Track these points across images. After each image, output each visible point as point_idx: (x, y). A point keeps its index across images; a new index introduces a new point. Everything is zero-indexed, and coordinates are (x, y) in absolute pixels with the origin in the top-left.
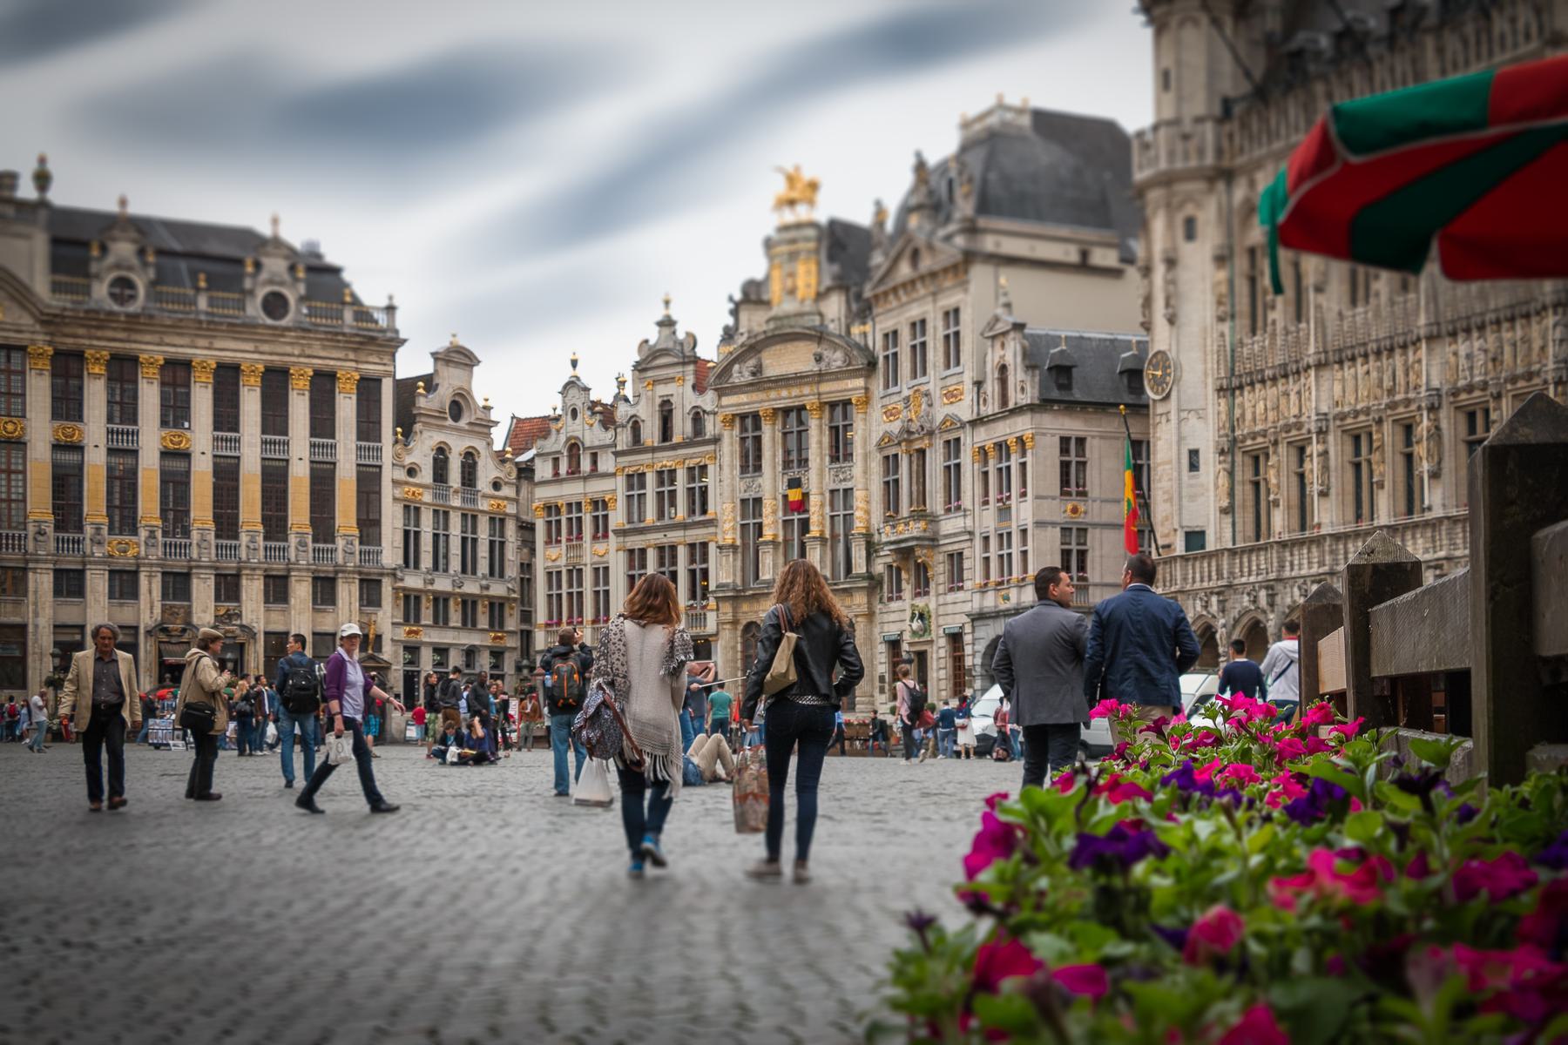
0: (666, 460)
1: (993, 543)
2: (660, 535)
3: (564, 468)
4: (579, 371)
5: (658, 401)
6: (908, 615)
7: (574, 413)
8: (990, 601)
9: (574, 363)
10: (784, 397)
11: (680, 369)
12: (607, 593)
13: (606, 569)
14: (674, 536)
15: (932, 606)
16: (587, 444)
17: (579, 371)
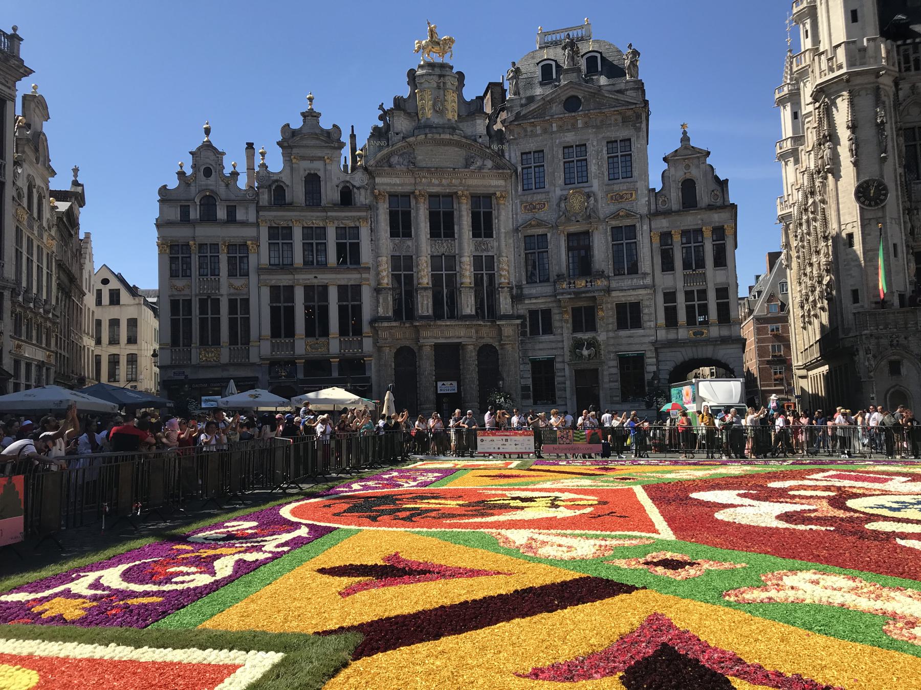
0: (314, 218)
1: (681, 299)
2: (312, 276)
3: (194, 214)
4: (211, 138)
5: (303, 174)
6: (567, 344)
7: (208, 172)
8: (683, 333)
9: (207, 131)
10: (436, 185)
11: (329, 151)
12: (247, 321)
13: (246, 302)
14: (323, 278)
15: (602, 337)
16: (223, 196)
17: (211, 138)
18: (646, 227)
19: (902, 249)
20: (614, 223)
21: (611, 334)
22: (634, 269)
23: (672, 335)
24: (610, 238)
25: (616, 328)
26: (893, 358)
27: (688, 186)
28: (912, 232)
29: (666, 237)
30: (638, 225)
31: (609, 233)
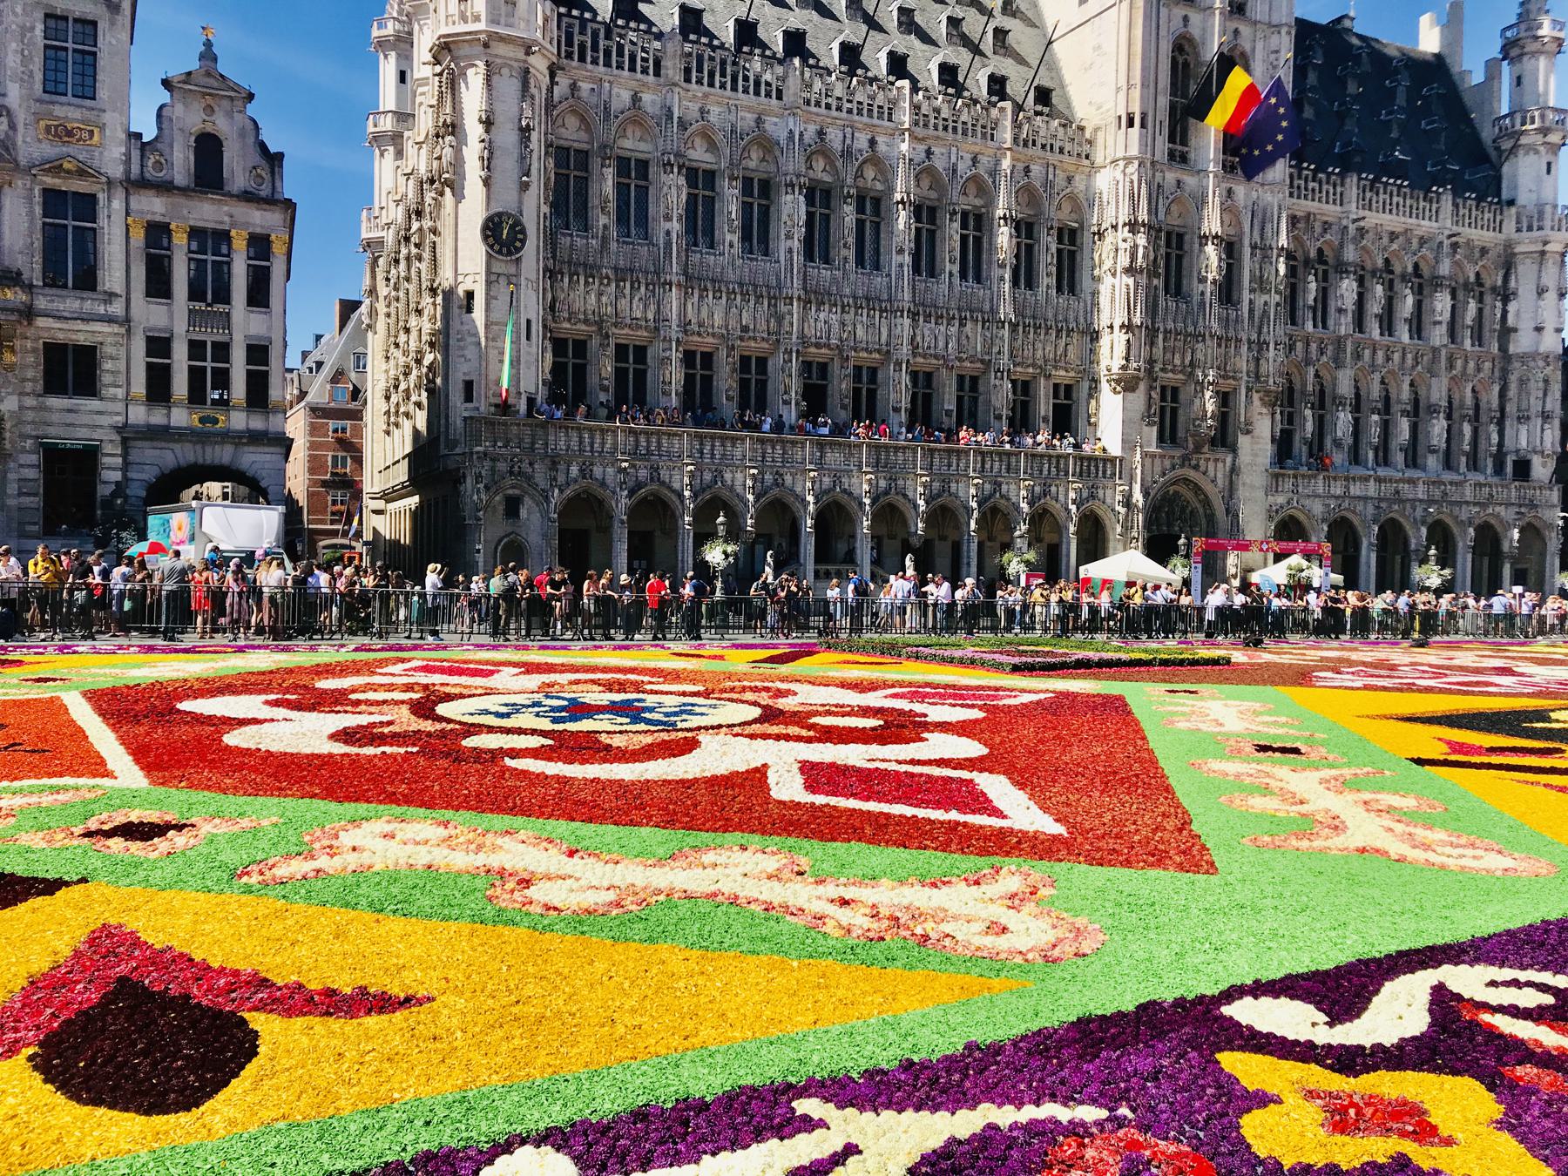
1: (180, 352)
8: (181, 417)
18: (118, 204)
19: (537, 328)
20: (51, 181)
21: (30, 402)
22: (87, 280)
23: (158, 417)
24: (38, 210)
25: (40, 387)
26: (510, 492)
27: (208, 148)
28: (552, 308)
29: (157, 232)
30: (101, 196)
31: (38, 199)
